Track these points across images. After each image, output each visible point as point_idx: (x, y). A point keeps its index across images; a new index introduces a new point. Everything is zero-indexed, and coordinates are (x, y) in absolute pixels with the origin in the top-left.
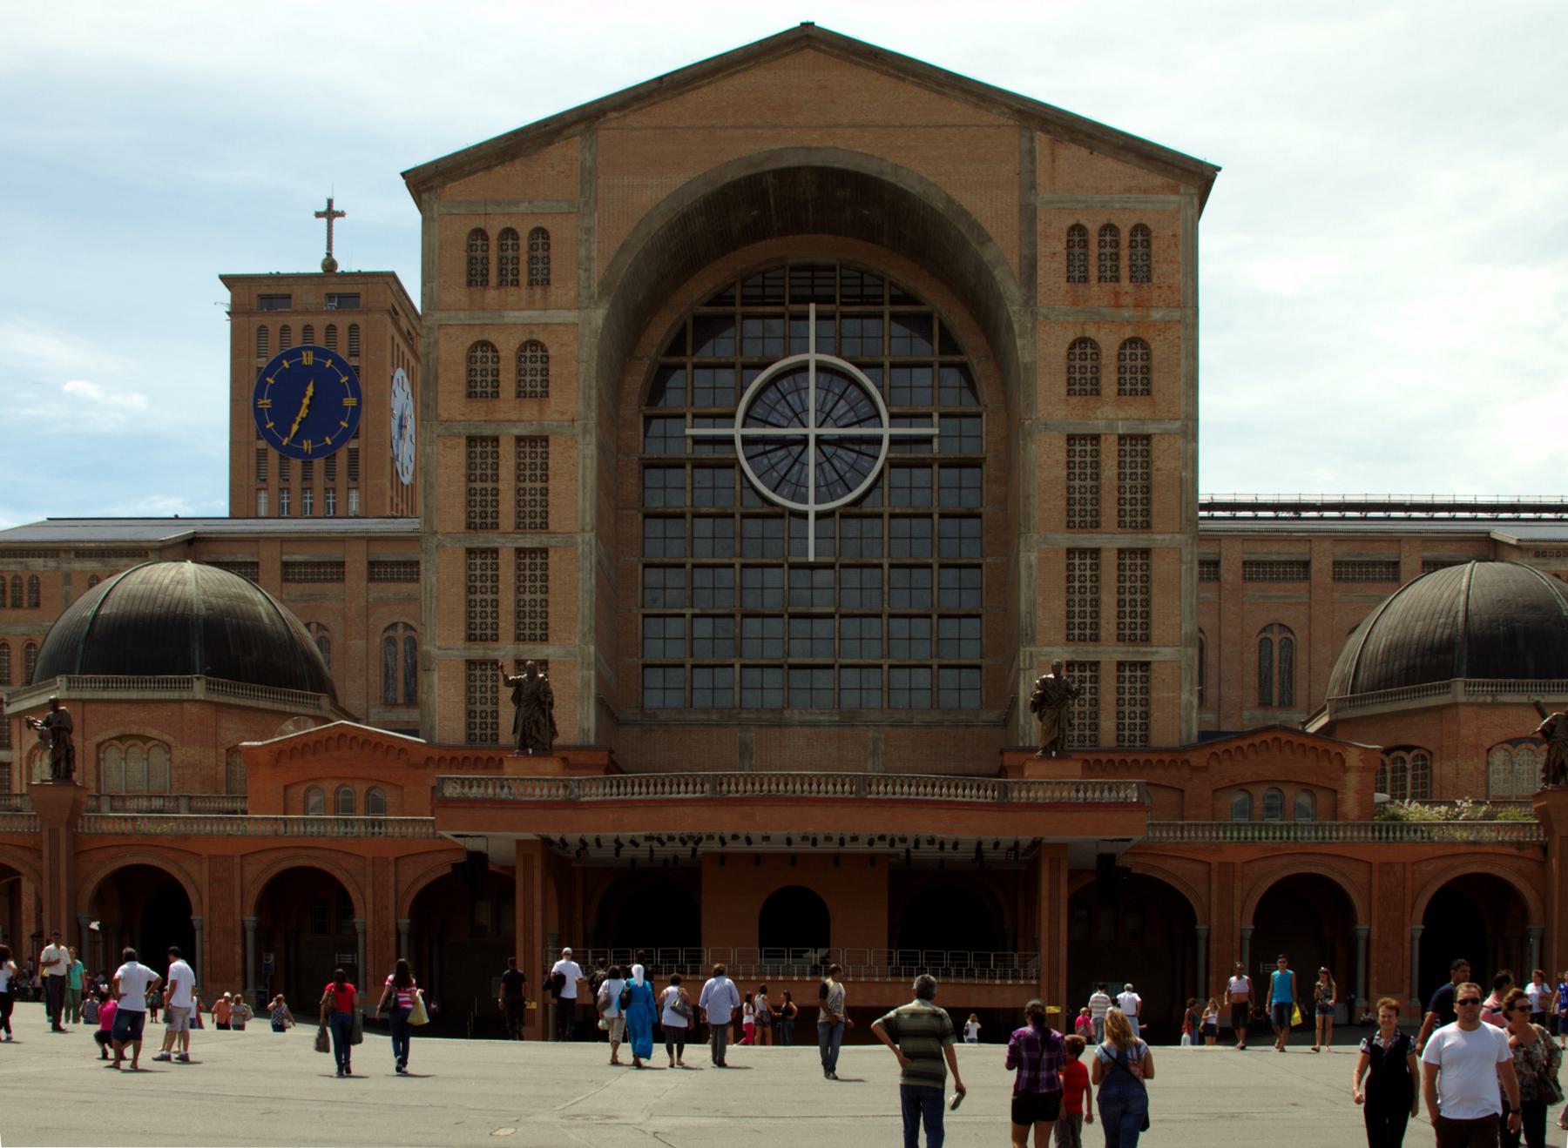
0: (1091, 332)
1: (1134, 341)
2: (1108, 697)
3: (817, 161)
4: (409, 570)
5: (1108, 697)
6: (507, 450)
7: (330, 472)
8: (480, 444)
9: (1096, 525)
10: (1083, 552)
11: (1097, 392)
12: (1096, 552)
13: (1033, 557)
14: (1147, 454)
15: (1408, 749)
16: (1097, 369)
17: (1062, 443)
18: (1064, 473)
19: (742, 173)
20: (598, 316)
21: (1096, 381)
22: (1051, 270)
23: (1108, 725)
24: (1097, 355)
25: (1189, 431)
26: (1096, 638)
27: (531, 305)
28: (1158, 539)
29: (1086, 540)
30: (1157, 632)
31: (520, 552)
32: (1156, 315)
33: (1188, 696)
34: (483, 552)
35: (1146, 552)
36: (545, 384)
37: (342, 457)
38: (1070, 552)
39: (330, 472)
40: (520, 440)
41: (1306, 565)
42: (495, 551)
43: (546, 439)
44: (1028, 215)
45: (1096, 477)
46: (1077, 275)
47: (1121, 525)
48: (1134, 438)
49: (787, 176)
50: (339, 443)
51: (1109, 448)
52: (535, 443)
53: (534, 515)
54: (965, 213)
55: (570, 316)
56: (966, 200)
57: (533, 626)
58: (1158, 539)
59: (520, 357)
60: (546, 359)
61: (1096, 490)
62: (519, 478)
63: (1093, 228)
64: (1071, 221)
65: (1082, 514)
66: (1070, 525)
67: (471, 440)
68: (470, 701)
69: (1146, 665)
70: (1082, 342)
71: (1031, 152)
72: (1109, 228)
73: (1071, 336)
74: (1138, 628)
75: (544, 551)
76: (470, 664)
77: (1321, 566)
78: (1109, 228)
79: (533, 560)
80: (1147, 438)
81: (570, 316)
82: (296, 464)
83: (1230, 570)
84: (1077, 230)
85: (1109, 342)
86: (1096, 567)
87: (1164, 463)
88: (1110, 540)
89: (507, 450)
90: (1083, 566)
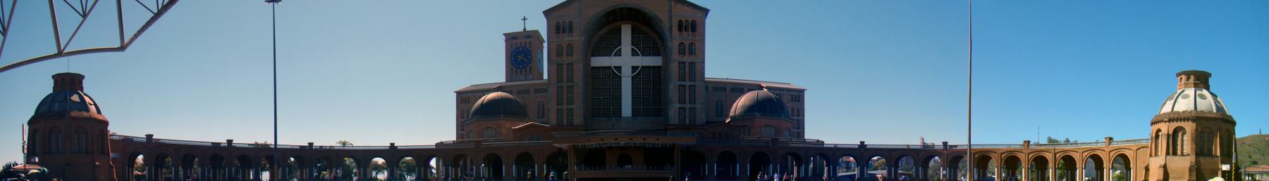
0: (683, 41)
1: (692, 44)
2: (687, 114)
3: (628, 6)
4: (545, 91)
5: (687, 114)
6: (565, 66)
7: (526, 71)
8: (560, 66)
9: (684, 80)
10: (682, 86)
11: (684, 54)
12: (684, 86)
13: (672, 86)
14: (695, 66)
15: (746, 126)
16: (684, 49)
17: (677, 65)
18: (678, 69)
19: (613, 9)
20: (583, 38)
21: (685, 52)
22: (675, 30)
23: (687, 120)
24: (684, 46)
25: (703, 62)
26: (685, 103)
27: (569, 37)
28: (697, 83)
29: (682, 83)
30: (697, 102)
31: (568, 87)
32: (697, 38)
33: (703, 115)
34: (560, 87)
35: (694, 86)
36: (572, 52)
37: (528, 68)
38: (679, 86)
39: (526, 71)
40: (567, 64)
41: (725, 88)
42: (563, 87)
43: (572, 64)
44: (670, 17)
45: (685, 70)
46: (680, 29)
47: (690, 80)
48: (692, 63)
49: (621, 9)
50: (527, 65)
51: (687, 65)
52: (570, 65)
53: (570, 79)
54: (658, 17)
55: (576, 38)
56: (658, 14)
57: (570, 102)
58: (697, 83)
59: (567, 48)
60: (573, 48)
61: (685, 73)
62: (567, 72)
63: (683, 21)
64: (679, 19)
65: (682, 78)
66: (679, 80)
67: (558, 64)
68: (557, 117)
69: (695, 108)
70: (682, 43)
71: (671, 5)
72: (687, 21)
73: (680, 42)
74: (693, 101)
75: (572, 86)
76: (558, 110)
77: (728, 88)
78: (687, 21)
79: (570, 89)
80: (695, 63)
81: (576, 38)
82: (519, 70)
83: (710, 89)
84: (680, 22)
85: (687, 43)
86: (685, 89)
87: (698, 68)
88: (687, 83)
89: (565, 66)
90: (682, 89)
